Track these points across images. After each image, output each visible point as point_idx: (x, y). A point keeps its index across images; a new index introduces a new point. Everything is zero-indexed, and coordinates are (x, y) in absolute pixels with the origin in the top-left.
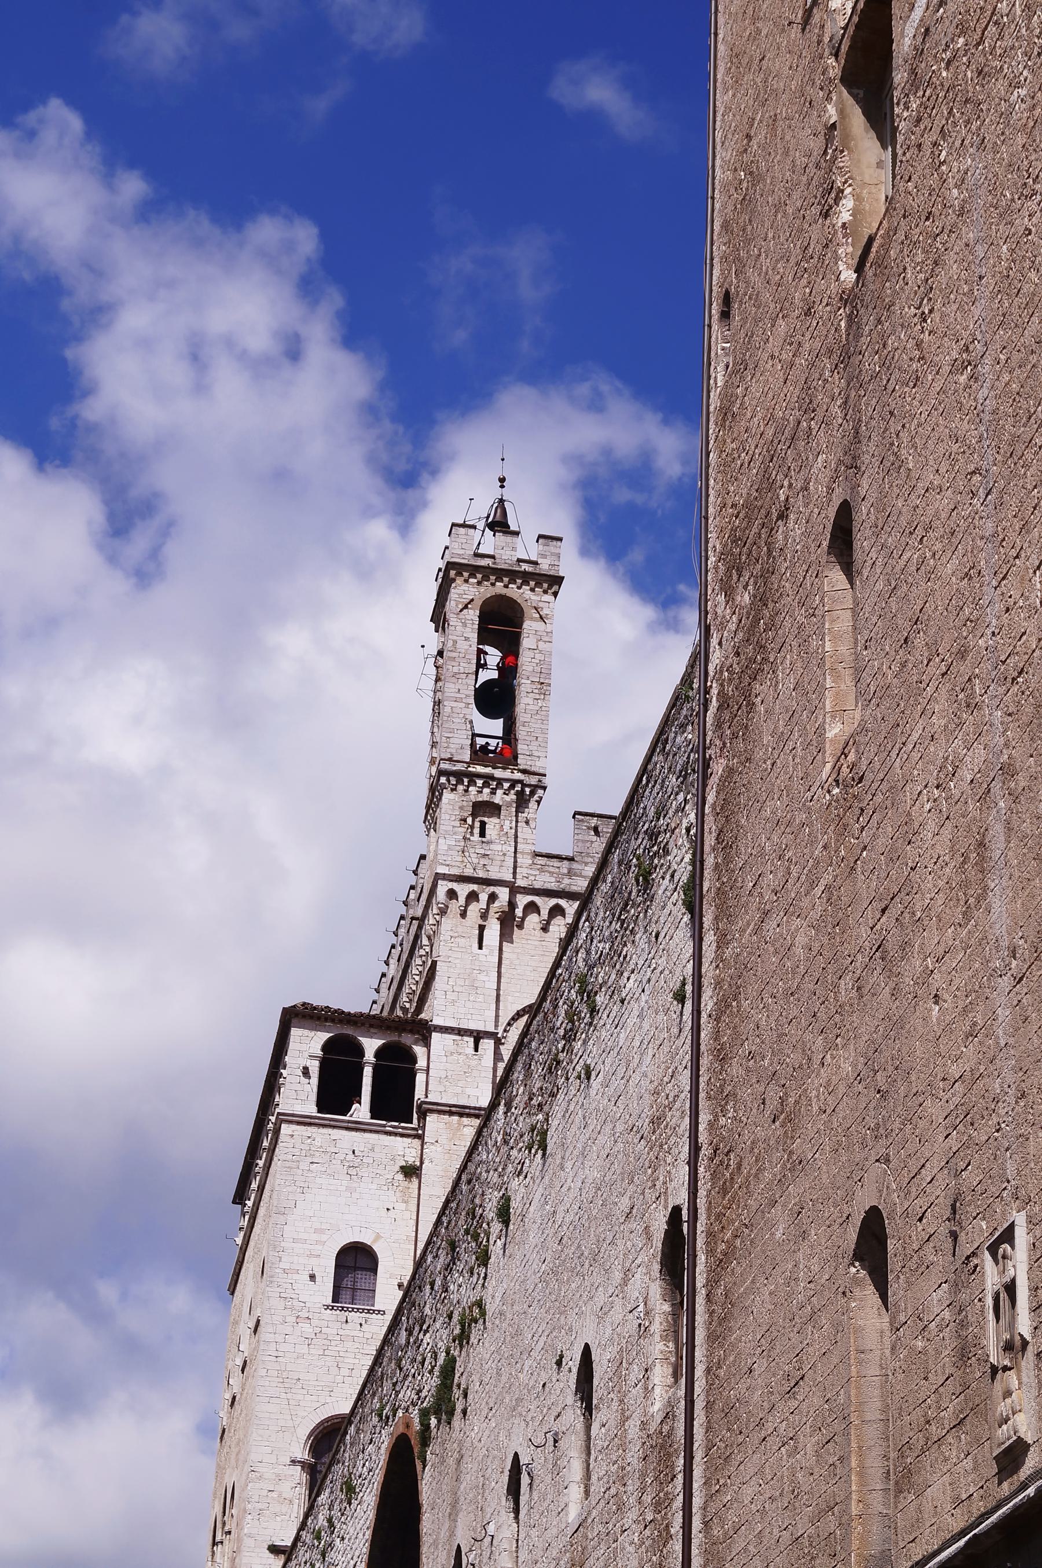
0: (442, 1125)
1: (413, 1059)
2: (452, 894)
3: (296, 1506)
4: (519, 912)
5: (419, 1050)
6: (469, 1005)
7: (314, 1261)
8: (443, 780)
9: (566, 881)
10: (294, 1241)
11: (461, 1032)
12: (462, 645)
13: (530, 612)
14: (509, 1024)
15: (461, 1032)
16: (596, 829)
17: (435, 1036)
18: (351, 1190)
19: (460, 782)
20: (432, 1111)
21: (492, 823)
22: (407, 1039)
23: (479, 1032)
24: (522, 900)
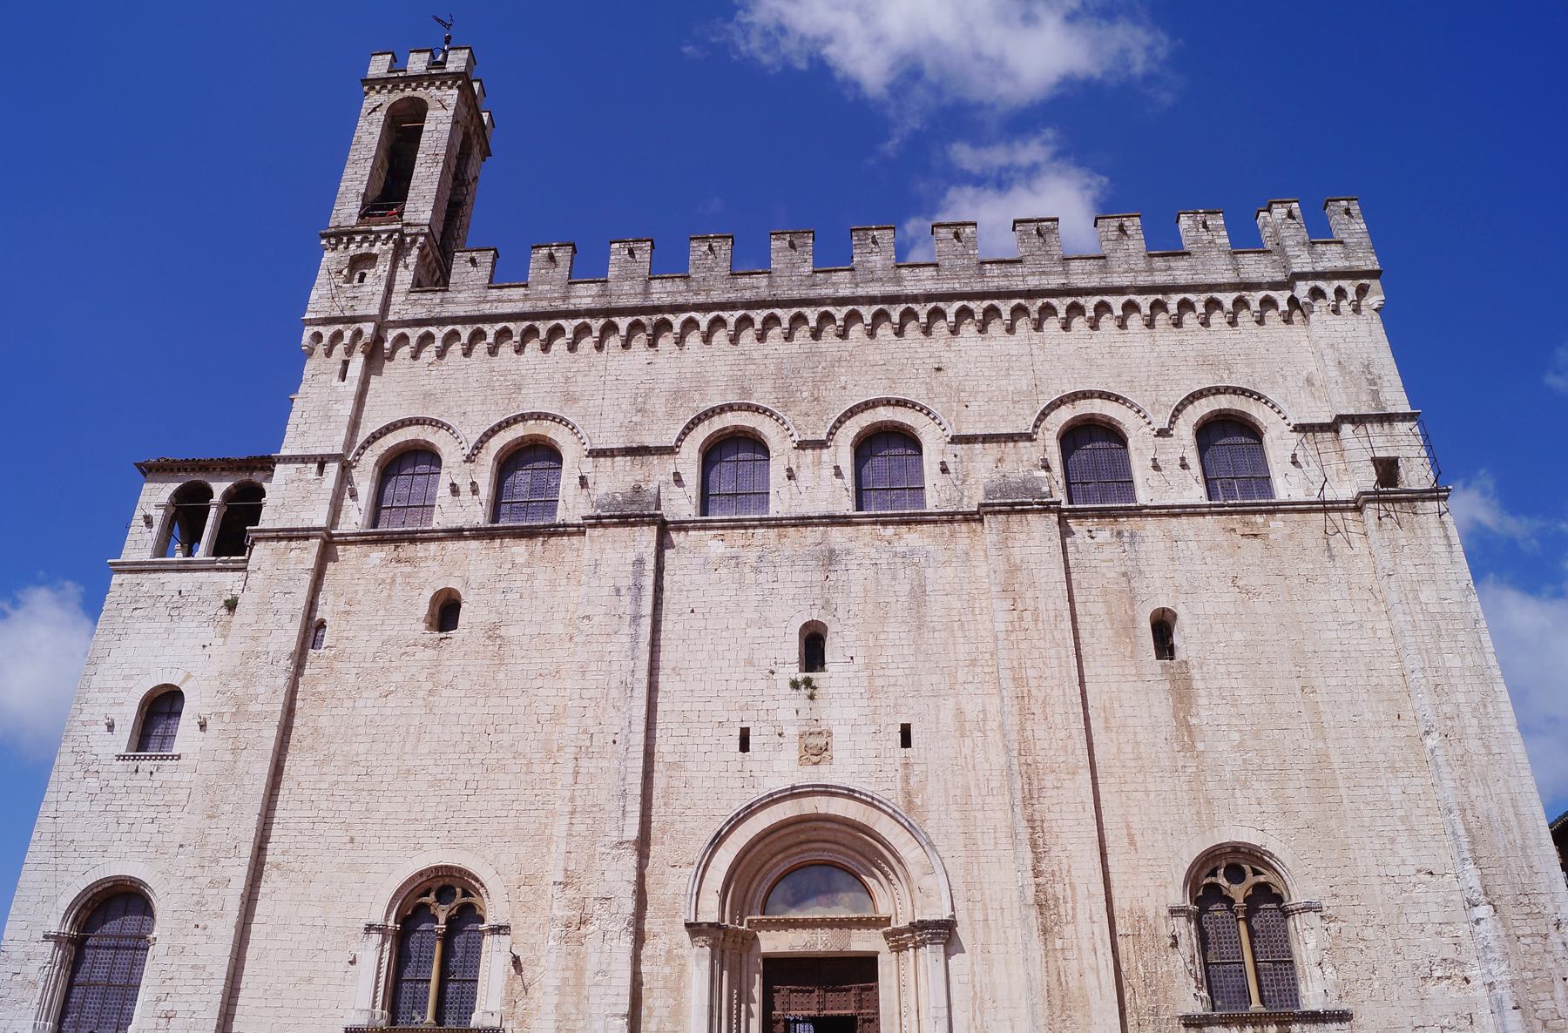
0: (268, 552)
1: (262, 493)
2: (318, 337)
3: (40, 991)
4: (387, 345)
6: (320, 433)
7: (117, 709)
8: (324, 242)
9: (438, 309)
10: (100, 690)
11: (304, 459)
12: (366, 138)
13: (431, 103)
14: (363, 447)
15: (304, 459)
16: (473, 261)
17: (279, 468)
18: (168, 631)
19: (339, 242)
20: (259, 539)
21: (370, 273)
22: (257, 477)
23: (322, 456)
24: (392, 334)
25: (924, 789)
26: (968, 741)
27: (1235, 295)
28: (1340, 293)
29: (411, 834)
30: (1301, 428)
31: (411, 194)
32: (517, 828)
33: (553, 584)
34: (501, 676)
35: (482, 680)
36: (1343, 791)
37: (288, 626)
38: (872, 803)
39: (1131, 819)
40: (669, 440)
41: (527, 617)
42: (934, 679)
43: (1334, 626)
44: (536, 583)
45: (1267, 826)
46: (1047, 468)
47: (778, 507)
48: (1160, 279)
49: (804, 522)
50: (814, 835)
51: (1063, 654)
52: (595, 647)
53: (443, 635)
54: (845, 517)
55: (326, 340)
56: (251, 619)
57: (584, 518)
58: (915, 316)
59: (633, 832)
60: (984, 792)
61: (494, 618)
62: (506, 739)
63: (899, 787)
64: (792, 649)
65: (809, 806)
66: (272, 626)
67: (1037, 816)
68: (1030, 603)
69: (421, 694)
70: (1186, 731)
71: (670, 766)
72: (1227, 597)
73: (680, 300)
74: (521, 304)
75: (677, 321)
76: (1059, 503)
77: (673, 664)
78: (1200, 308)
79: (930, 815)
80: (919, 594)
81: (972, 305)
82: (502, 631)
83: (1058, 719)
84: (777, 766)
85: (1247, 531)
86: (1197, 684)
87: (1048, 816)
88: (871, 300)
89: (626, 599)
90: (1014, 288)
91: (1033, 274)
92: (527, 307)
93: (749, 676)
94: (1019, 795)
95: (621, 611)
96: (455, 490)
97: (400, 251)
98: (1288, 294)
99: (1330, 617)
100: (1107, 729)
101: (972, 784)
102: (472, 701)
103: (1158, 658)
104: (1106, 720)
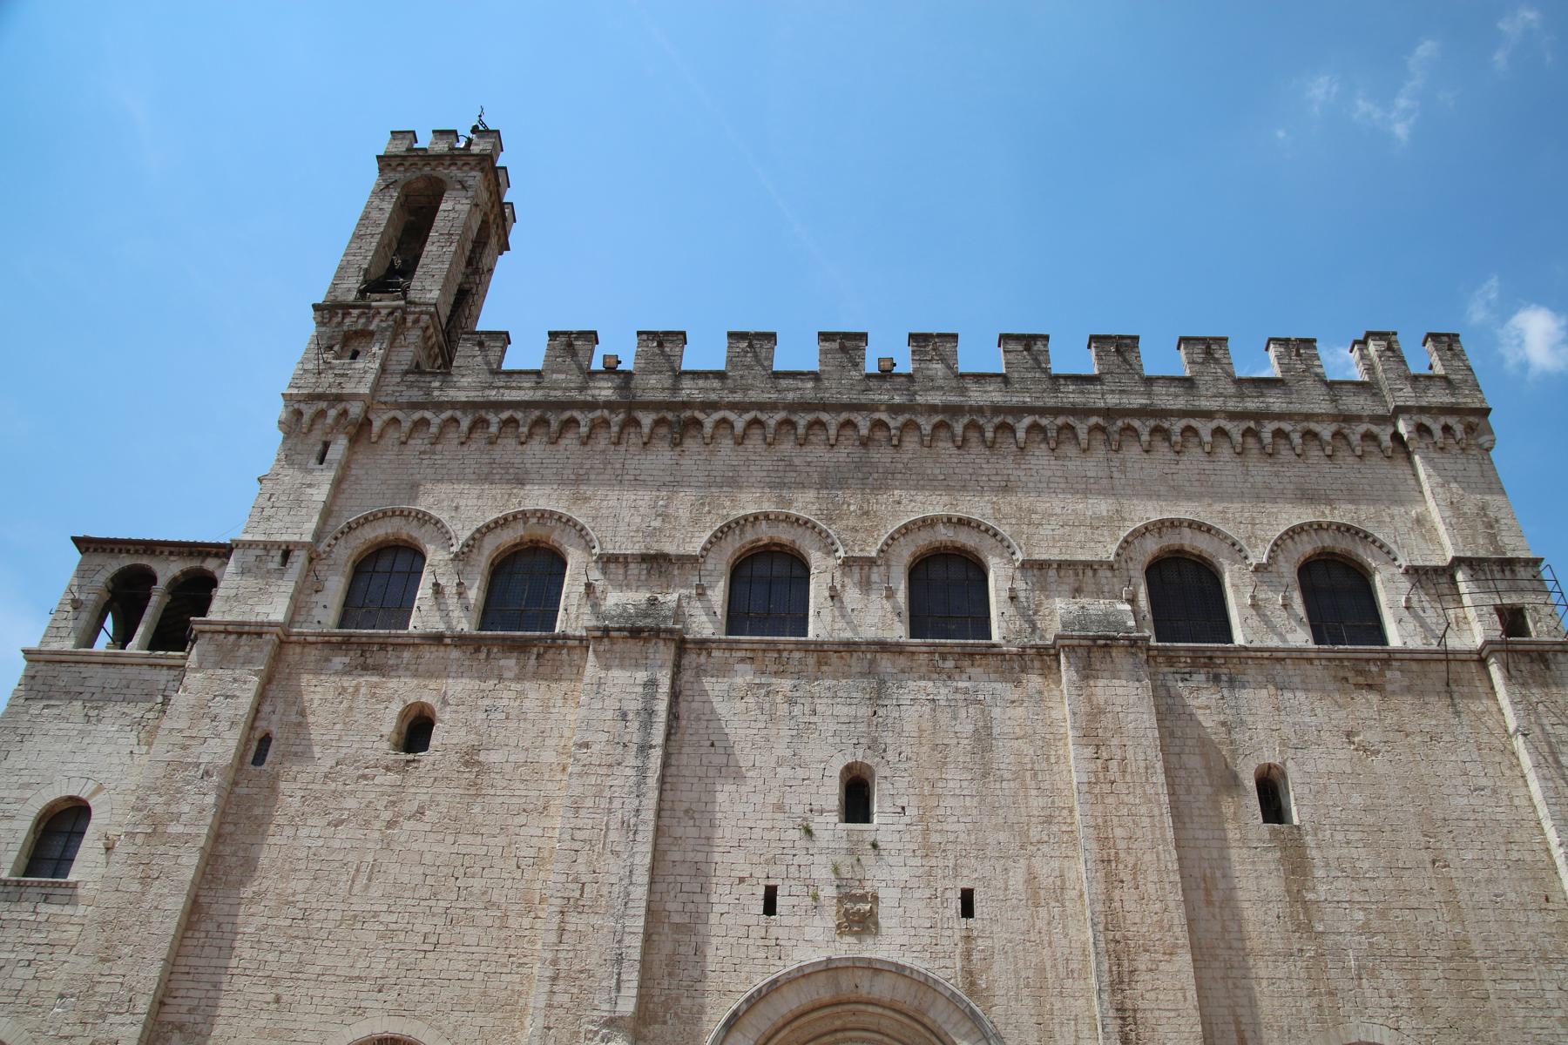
0: (212, 648)
5: (217, 574)
6: (288, 519)
15: (267, 546)
22: (210, 565)
23: (288, 544)
25: (989, 968)
26: (1043, 912)
27: (1334, 427)
28: (1447, 429)
29: (352, 995)
30: (1419, 575)
31: (419, 272)
32: (485, 994)
33: (546, 707)
34: (476, 809)
35: (454, 813)
36: (1489, 985)
37: (227, 735)
38: (926, 984)
39: (1239, 1011)
40: (694, 547)
41: (513, 742)
42: (1002, 836)
43: (1463, 790)
44: (527, 703)
45: (1402, 1025)
46: (1132, 601)
47: (816, 629)
48: (1252, 405)
49: (849, 647)
50: (851, 1020)
51: (1156, 812)
52: (593, 780)
53: (410, 756)
54: (898, 644)
55: (306, 418)
56: (183, 723)
57: (587, 629)
58: (981, 429)
59: (627, 1006)
60: (1062, 972)
61: (473, 739)
62: (477, 884)
63: (959, 965)
64: (832, 794)
65: (846, 982)
66: (207, 734)
67: (1129, 1004)
68: (1118, 754)
69: (377, 825)
70: (1301, 911)
71: (678, 928)
72: (1340, 754)
73: (713, 397)
74: (531, 393)
75: (709, 421)
76: (1147, 639)
77: (685, 805)
78: (1296, 439)
79: (996, 1000)
80: (984, 738)
81: (1044, 422)
82: (482, 757)
83: (1151, 888)
84: (809, 933)
85: (1361, 680)
86: (1314, 853)
87: (1140, 1004)
88: (932, 409)
89: (634, 725)
90: (1091, 405)
91: (1112, 392)
92: (539, 395)
93: (779, 824)
94: (1106, 978)
95: (627, 738)
96: (437, 589)
97: (399, 327)
98: (1390, 430)
99: (1459, 781)
100: (1209, 903)
101: (1048, 964)
102: (440, 837)
103: (1267, 819)
104: (1208, 892)
